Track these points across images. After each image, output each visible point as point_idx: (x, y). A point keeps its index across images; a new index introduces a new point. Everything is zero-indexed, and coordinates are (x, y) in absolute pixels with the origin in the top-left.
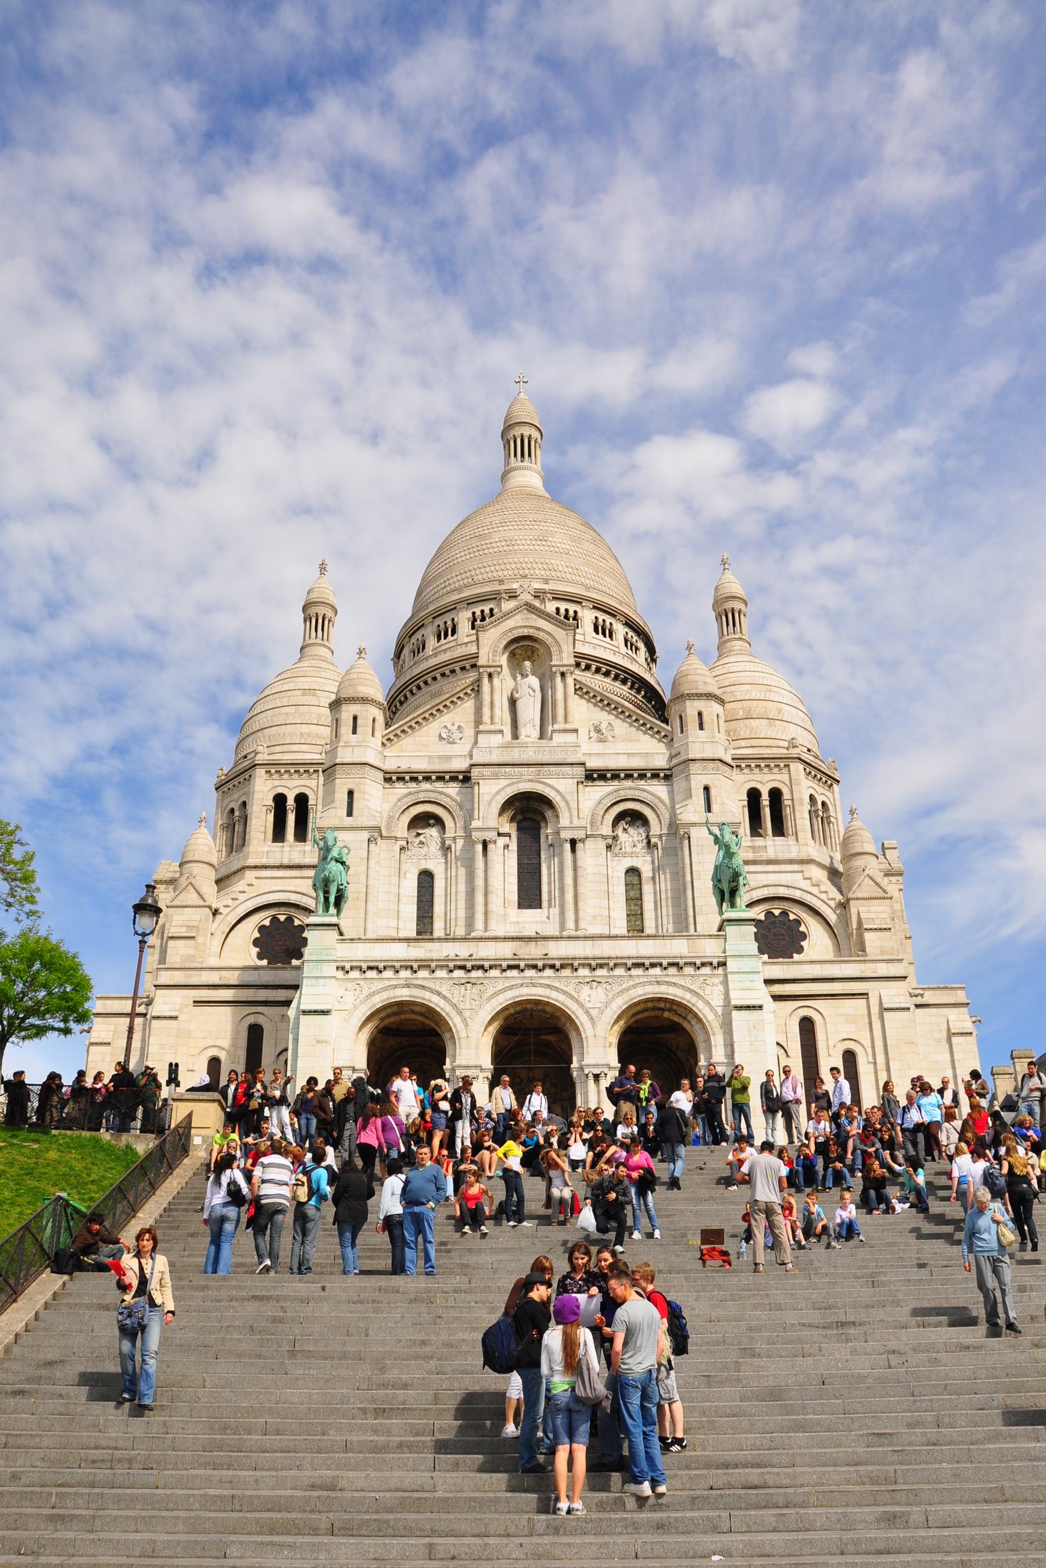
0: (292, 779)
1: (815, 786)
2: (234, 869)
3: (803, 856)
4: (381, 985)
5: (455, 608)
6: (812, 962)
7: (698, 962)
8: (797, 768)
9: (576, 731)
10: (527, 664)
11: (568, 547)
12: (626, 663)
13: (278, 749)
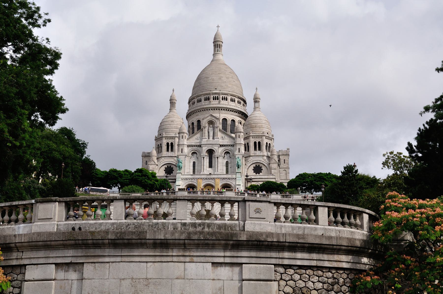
1: (268, 140)
2: (160, 157)
3: (263, 155)
9: (219, 138)
13: (167, 134)
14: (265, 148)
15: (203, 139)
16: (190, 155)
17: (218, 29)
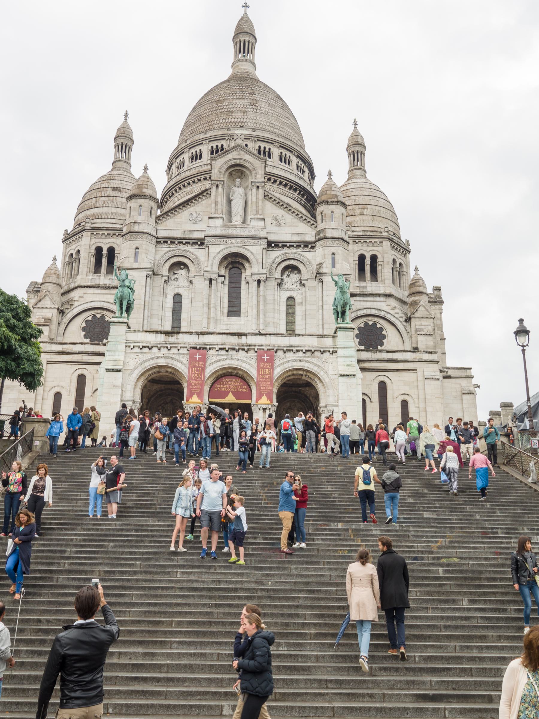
0: (106, 238)
1: (397, 254)
3: (388, 292)
4: (150, 356)
5: (202, 143)
6: (388, 352)
7: (322, 350)
8: (387, 244)
9: (263, 219)
10: (238, 180)
11: (267, 110)
12: (297, 180)
14: (391, 274)
15: (211, 220)
16: (165, 271)
17: (246, 10)
